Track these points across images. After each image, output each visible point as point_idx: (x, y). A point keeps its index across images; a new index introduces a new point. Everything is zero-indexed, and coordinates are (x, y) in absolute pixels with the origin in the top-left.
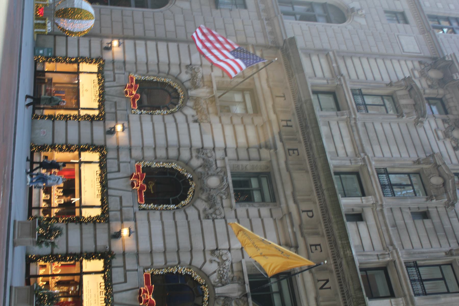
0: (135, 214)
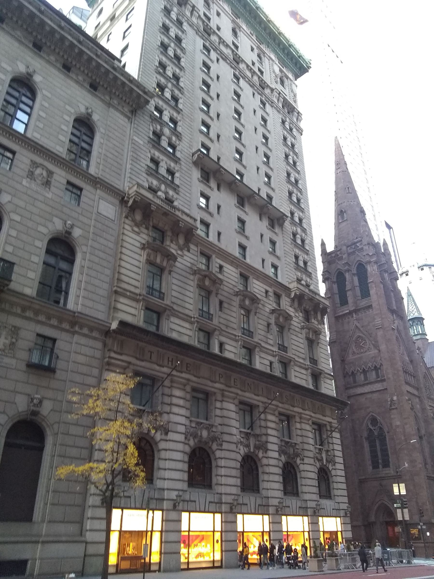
0: (217, 493)
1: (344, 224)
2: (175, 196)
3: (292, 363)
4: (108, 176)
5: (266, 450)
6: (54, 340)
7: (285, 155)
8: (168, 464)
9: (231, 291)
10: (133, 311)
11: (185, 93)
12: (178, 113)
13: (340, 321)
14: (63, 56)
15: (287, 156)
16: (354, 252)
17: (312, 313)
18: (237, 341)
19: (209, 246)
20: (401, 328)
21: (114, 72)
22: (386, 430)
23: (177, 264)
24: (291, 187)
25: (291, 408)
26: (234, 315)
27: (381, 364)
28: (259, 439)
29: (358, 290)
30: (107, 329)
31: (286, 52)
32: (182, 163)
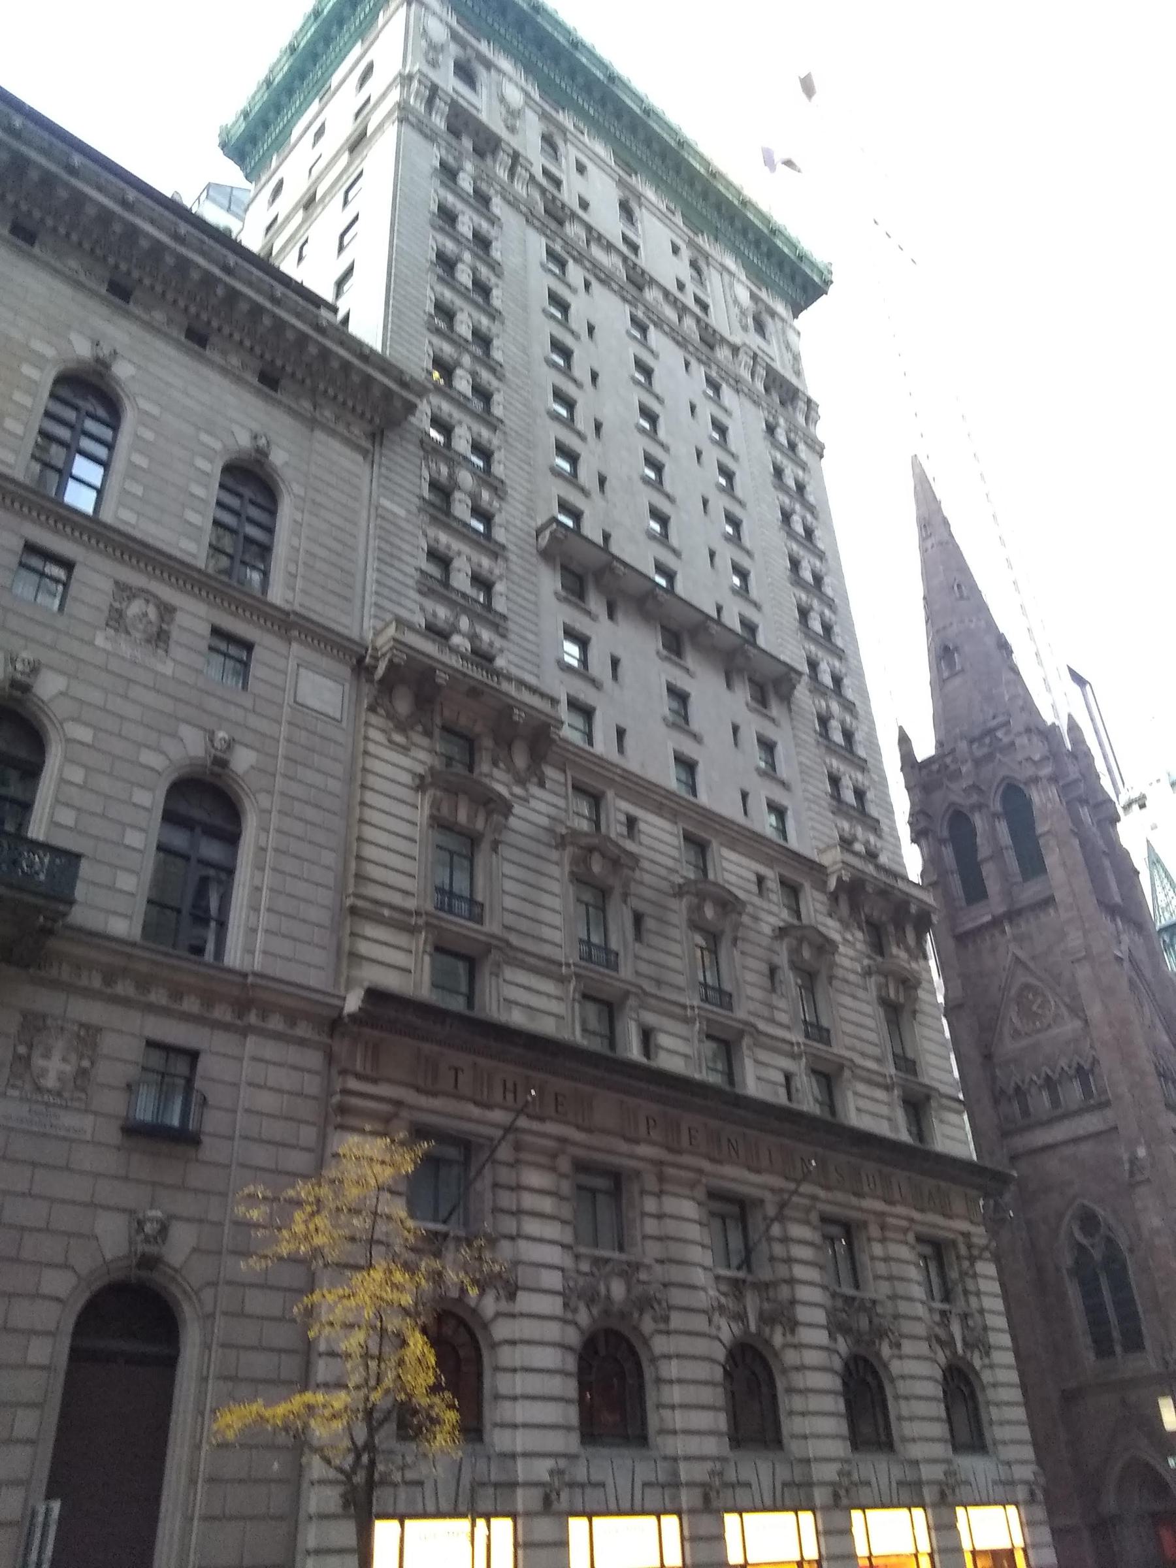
1: (957, 681)
2: (499, 643)
3: (847, 1074)
4: (319, 607)
5: (793, 1325)
6: (193, 1056)
7: (782, 514)
8: (521, 1384)
9: (664, 885)
10: (400, 958)
11: (508, 375)
12: (494, 429)
13: (970, 946)
14: (186, 309)
15: (786, 517)
16: (989, 757)
17: (891, 929)
18: (687, 1021)
19: (597, 769)
20: (1141, 955)
21: (320, 339)
22: (1123, 1243)
23: (513, 822)
24: (804, 597)
25: (854, 1201)
26: (676, 948)
27: (1094, 1057)
28: (771, 1294)
29: (1011, 857)
30: (335, 1014)
31: (764, 248)
32: (513, 557)
